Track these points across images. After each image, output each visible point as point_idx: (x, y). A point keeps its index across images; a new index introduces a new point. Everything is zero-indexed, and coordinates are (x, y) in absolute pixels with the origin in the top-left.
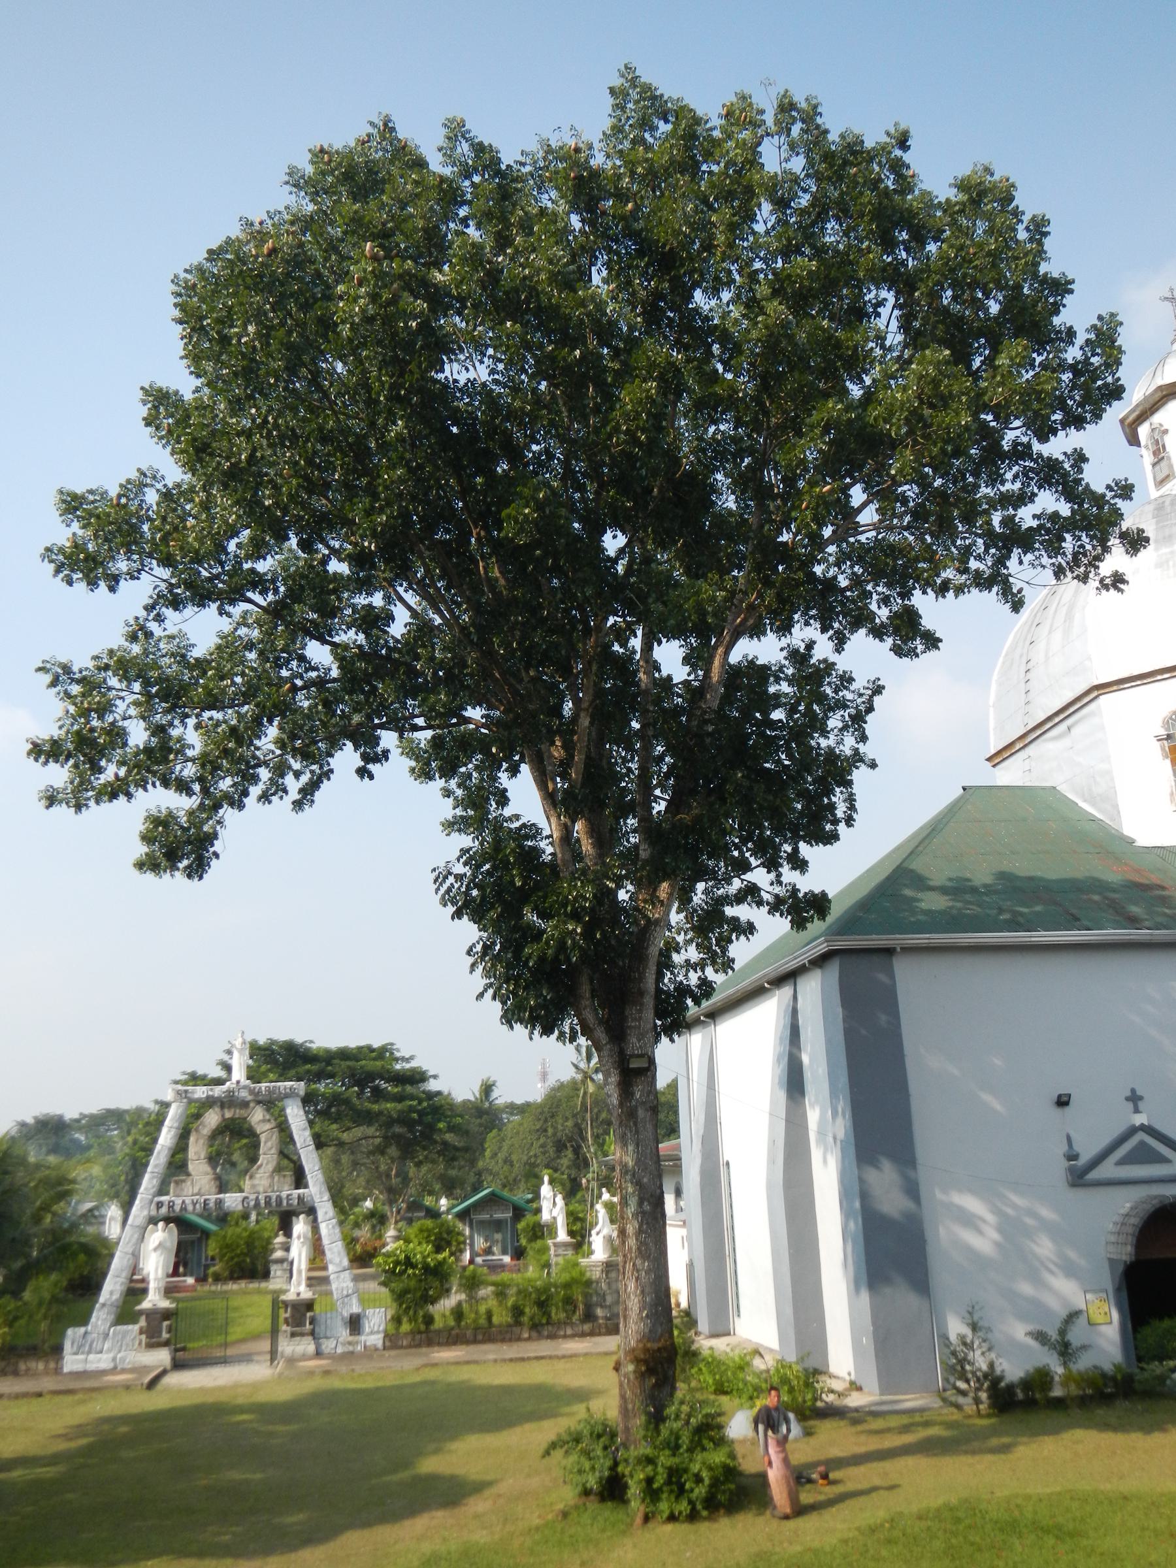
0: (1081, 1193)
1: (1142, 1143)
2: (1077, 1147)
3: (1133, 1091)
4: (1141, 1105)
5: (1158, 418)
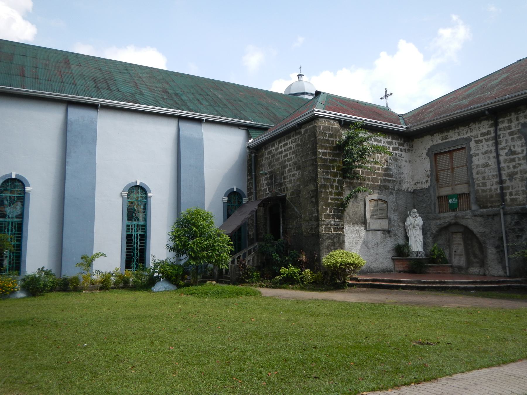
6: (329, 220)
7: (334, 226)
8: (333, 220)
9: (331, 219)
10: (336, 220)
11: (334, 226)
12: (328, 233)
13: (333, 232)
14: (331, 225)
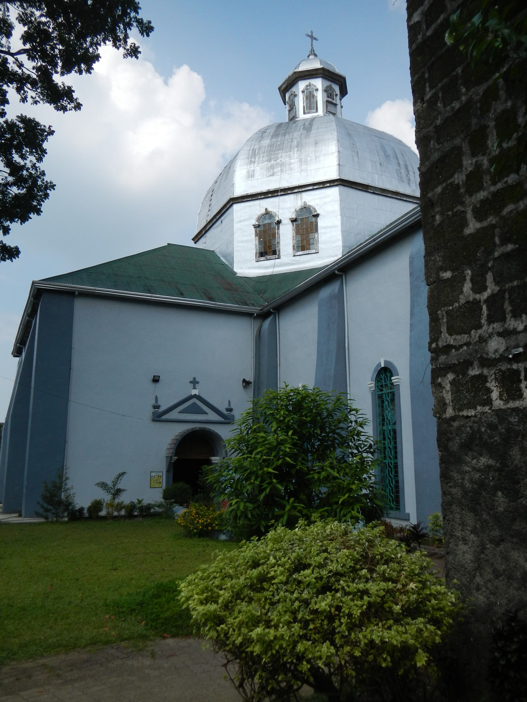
0: (158, 424)
1: (194, 404)
2: (159, 403)
3: (194, 378)
4: (197, 385)
5: (294, 89)
6: (475, 334)
7: (504, 367)
8: (497, 326)
9: (486, 329)
10: (512, 323)
11: (504, 367)
12: (472, 413)
13: (498, 404)
14: (486, 362)
